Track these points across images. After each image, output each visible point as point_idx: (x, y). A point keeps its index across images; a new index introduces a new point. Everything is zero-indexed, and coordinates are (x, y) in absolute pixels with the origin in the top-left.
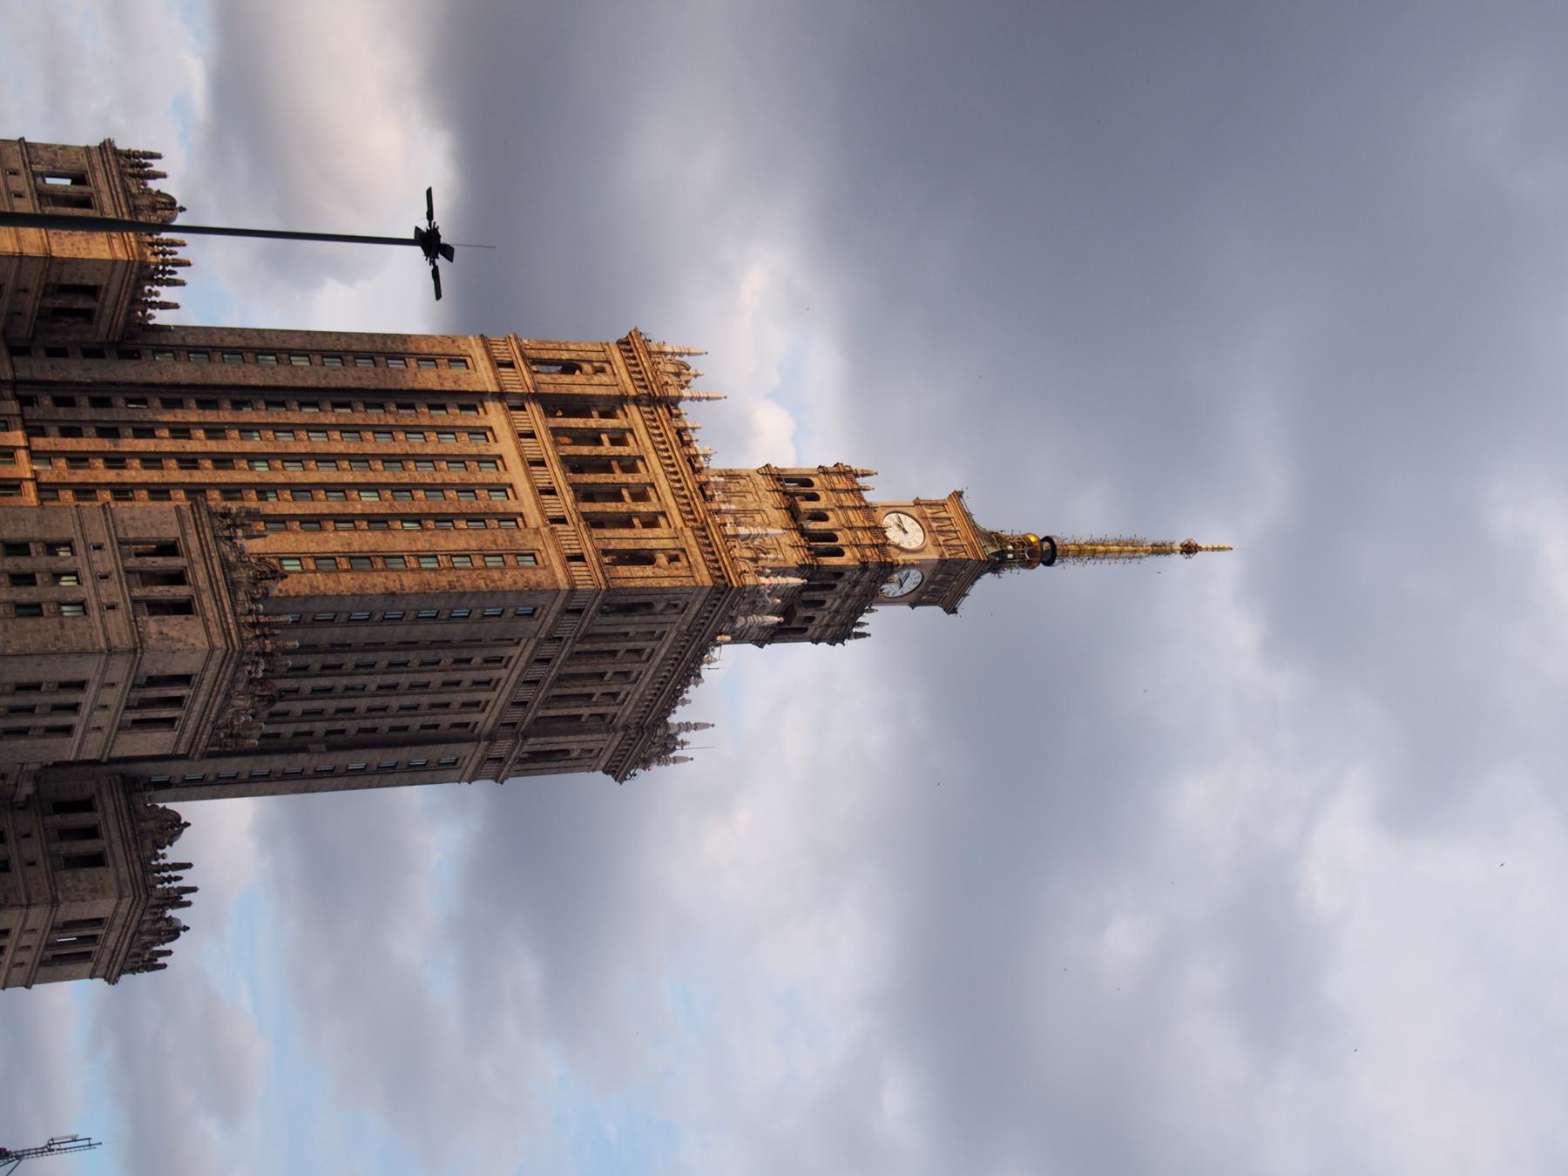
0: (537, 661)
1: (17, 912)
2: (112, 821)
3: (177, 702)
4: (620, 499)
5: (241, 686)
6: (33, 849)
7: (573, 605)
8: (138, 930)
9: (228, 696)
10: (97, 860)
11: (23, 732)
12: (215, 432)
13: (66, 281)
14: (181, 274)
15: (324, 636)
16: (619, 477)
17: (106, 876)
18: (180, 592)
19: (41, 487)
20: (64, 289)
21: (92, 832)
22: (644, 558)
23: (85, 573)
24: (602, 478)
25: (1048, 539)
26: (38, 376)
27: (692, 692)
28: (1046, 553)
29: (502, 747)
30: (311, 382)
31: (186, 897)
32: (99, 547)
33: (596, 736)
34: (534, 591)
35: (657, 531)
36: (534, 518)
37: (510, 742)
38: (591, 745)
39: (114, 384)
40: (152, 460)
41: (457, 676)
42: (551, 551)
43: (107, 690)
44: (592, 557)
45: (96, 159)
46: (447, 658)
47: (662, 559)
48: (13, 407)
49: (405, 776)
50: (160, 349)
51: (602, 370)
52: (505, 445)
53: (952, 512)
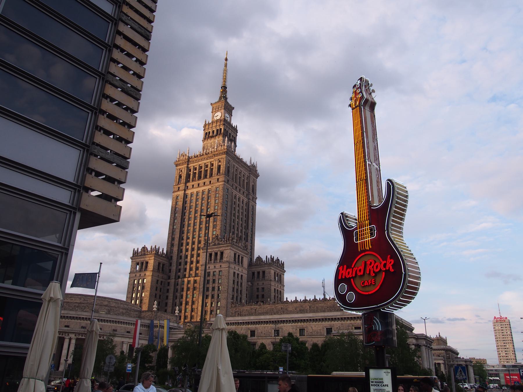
3: (239, 256)
4: (207, 170)
6: (260, 283)
8: (277, 266)
10: (264, 272)
11: (241, 283)
12: (187, 244)
14: (157, 247)
15: (228, 228)
16: (203, 170)
17: (267, 271)
18: (219, 254)
19: (195, 276)
20: (158, 269)
21: (259, 273)
22: (219, 167)
23: (214, 270)
24: (203, 173)
27: (244, 160)
28: (224, 88)
29: (251, 197)
30: (179, 225)
34: (223, 188)
36: (209, 187)
40: (192, 256)
44: (218, 177)
45: (134, 260)
46: (234, 206)
47: (220, 164)
48: (180, 280)
52: (195, 191)
53: (215, 106)
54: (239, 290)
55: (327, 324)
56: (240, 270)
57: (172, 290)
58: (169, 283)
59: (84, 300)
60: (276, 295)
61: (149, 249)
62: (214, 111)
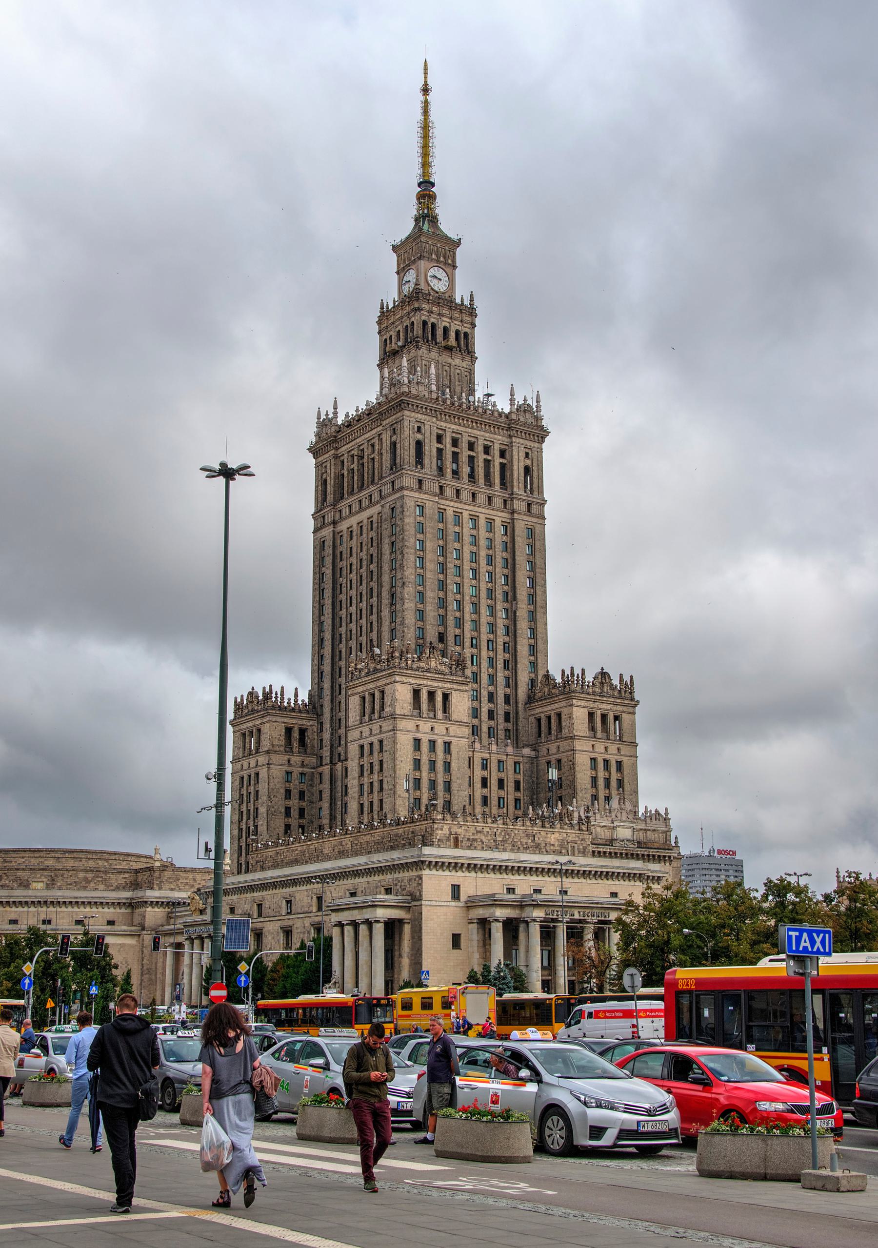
0: (458, 497)
1: (577, 755)
2: (545, 709)
3: (431, 695)
5: (422, 664)
6: (553, 750)
7: (416, 486)
9: (428, 670)
10: (559, 715)
11: (447, 766)
14: (276, 689)
17: (565, 712)
18: (377, 694)
24: (366, 469)
25: (419, 185)
31: (577, 671)
32: (361, 732)
33: (515, 453)
35: (384, 440)
36: (376, 509)
38: (522, 455)
39: (331, 718)
41: (467, 539)
42: (390, 499)
43: (420, 728)
46: (453, 545)
49: (538, 555)
50: (320, 697)
51: (326, 467)
52: (353, 521)
55: (350, 883)
57: (326, 795)
58: (321, 774)
60: (602, 774)
61: (261, 698)
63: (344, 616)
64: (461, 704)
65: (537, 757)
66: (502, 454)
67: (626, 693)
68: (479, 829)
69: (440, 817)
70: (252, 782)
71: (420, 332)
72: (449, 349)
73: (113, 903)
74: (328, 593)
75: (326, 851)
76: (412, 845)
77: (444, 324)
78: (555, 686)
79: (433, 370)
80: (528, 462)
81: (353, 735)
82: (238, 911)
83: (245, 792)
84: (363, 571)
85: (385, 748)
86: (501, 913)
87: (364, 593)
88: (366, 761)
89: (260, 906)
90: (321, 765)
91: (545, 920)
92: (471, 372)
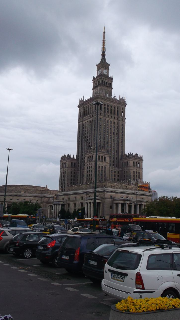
3: (102, 157)
5: (100, 151)
6: (126, 169)
7: (100, 114)
9: (102, 152)
10: (127, 162)
11: (105, 171)
13: (71, 166)
14: (70, 155)
17: (128, 161)
21: (125, 163)
23: (89, 166)
24: (89, 110)
25: (102, 52)
26: (80, 168)
29: (120, 119)
36: (91, 119)
37: (120, 118)
41: (110, 125)
42: (94, 117)
49: (124, 129)
51: (81, 111)
52: (86, 121)
54: (103, 174)
56: (104, 164)
57: (79, 176)
58: (78, 172)
59: (16, 187)
60: (135, 174)
62: (98, 70)
63: (84, 140)
64: (108, 159)
65: (122, 170)
66: (117, 108)
67: (141, 159)
68: (116, 184)
69: (108, 182)
70: (64, 173)
71: (102, 83)
72: (107, 86)
73: (38, 197)
74: (81, 136)
75: (83, 188)
76: (102, 187)
77: (106, 81)
78: (127, 156)
79: (104, 90)
80: (122, 110)
81: (86, 165)
82: (64, 199)
83: (62, 175)
84: (88, 131)
85: (92, 167)
86: (121, 202)
87: (88, 136)
88: (88, 170)
89: (69, 198)
90: (78, 170)
91: (130, 204)
92: (111, 91)
